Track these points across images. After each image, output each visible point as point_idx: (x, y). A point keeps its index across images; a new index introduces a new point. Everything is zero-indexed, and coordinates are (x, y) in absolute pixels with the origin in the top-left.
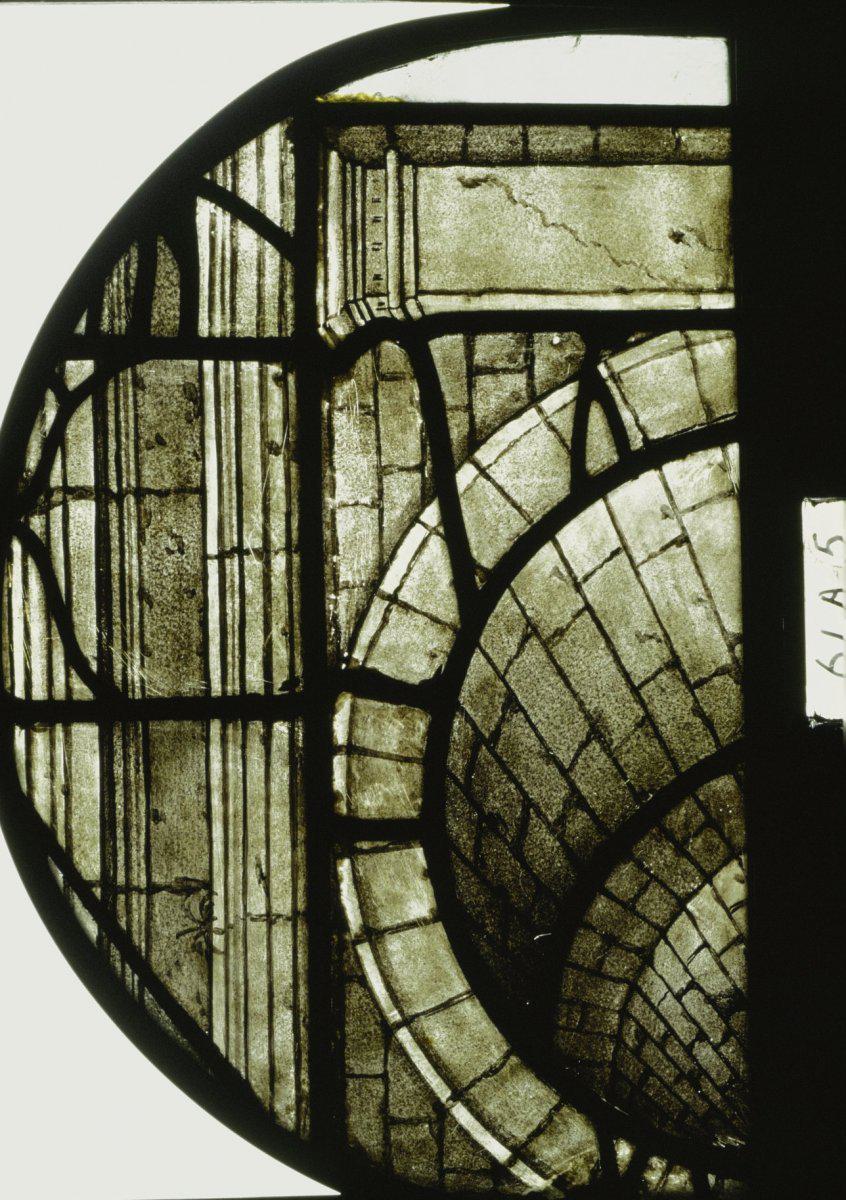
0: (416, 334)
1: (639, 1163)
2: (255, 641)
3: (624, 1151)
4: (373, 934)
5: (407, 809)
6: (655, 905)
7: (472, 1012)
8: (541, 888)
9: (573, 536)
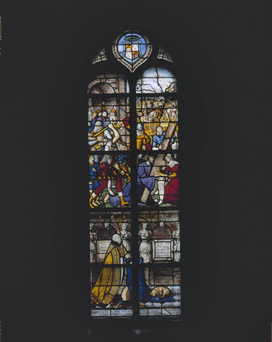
0: (118, 82)
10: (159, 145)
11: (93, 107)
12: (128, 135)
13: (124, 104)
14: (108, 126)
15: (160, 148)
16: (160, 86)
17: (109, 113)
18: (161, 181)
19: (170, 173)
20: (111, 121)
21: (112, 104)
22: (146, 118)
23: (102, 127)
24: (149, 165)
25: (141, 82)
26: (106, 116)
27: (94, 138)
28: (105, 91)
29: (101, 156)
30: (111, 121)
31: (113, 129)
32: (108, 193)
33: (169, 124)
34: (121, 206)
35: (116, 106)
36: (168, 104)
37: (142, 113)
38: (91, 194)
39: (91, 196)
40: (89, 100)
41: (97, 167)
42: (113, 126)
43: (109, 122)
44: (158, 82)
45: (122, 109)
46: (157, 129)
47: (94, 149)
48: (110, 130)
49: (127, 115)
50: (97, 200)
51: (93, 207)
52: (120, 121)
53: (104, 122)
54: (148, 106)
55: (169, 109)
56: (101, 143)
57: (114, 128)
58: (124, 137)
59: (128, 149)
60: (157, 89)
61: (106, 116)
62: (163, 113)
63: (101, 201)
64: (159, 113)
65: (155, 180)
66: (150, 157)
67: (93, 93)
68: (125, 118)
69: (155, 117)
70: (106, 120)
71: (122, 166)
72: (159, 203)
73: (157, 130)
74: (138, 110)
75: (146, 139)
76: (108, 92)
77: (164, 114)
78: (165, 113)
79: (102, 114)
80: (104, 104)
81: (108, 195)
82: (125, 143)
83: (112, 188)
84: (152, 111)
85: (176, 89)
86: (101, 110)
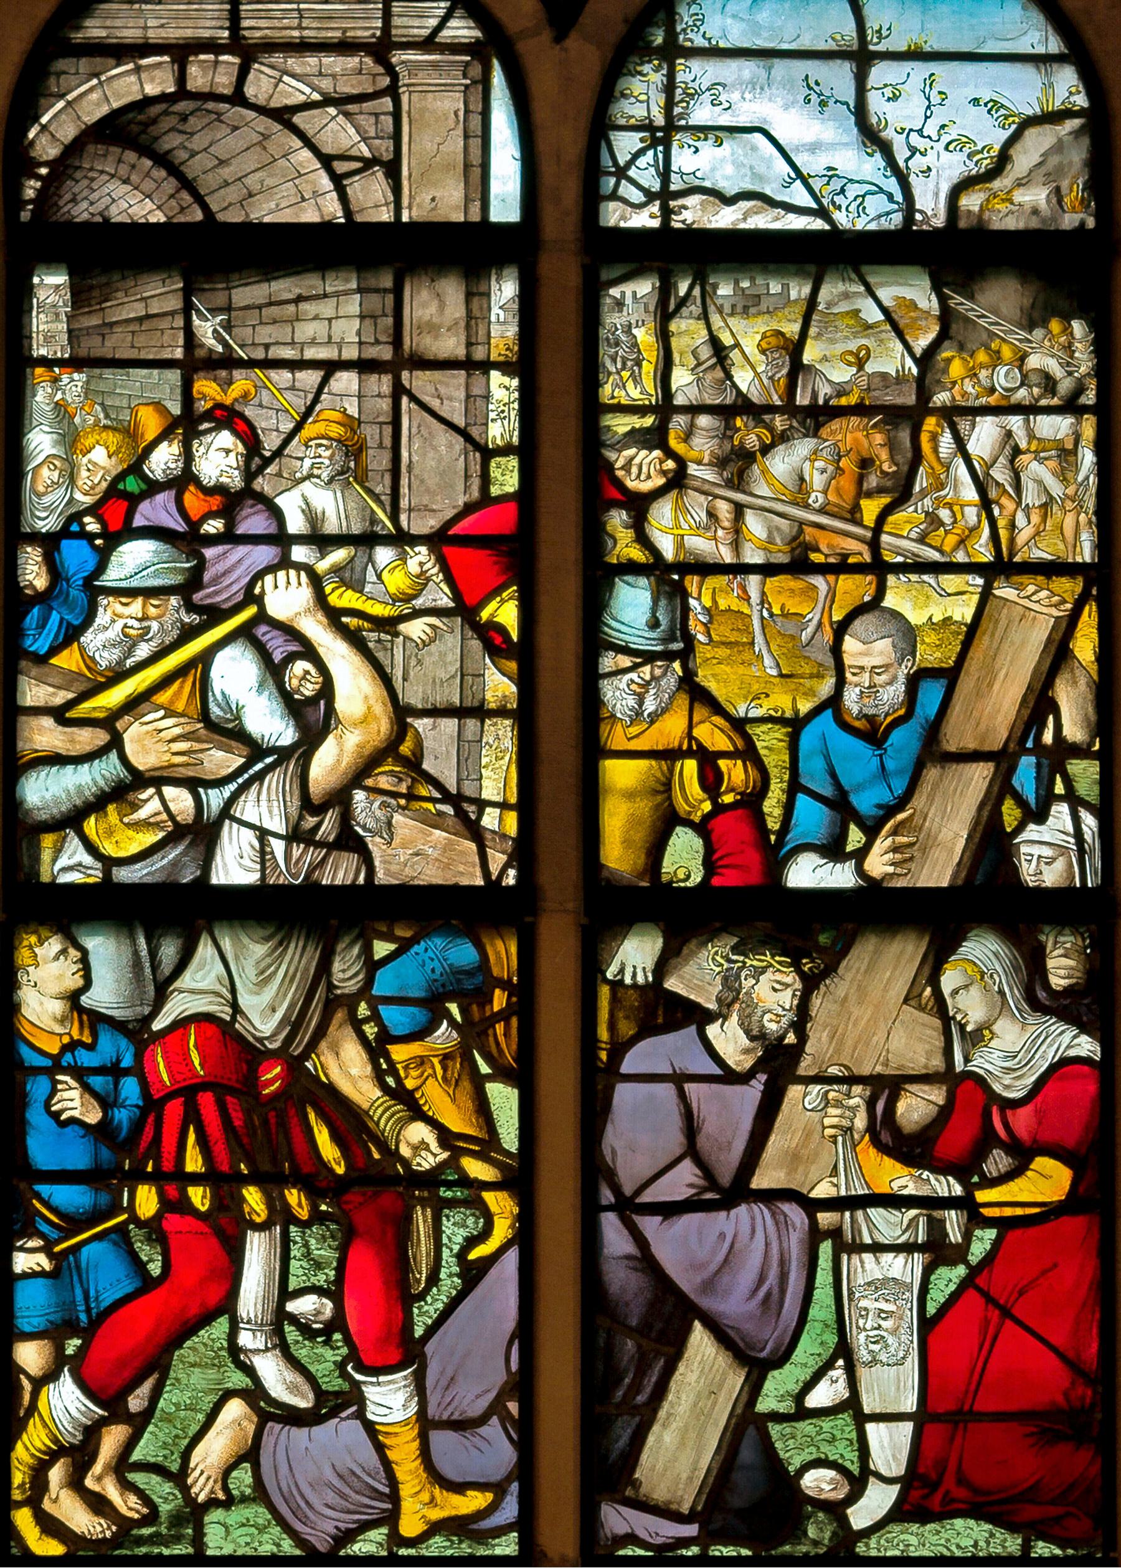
0: (393, 91)
1: (38, 177)
2: (262, 23)
3: (44, 171)
4: (138, 70)
5: (191, 86)
6: (148, 185)
7: (105, 110)
8: (157, 139)
9: (306, 154)
10: (872, 831)
11: (80, 377)
12: (501, 712)
13: (451, 346)
14: (259, 600)
15: (878, 864)
16: (886, 149)
17: (270, 443)
18: (887, 1258)
19: (998, 1161)
20: (300, 539)
21: (313, 342)
22: (712, 514)
23: (190, 607)
24: (748, 1062)
25: (658, 100)
26: (235, 481)
27: (89, 738)
28: (233, 194)
29: (169, 951)
30: (300, 539)
31: (315, 629)
32: (237, 1379)
33: (986, 595)
34: (396, 1539)
35: (364, 366)
36: (982, 357)
37: (670, 453)
38: (35, 1394)
39: (33, 1408)
40: (41, 294)
41: (115, 1071)
42: (321, 599)
43: (265, 554)
44: (860, 112)
45: (435, 404)
46: (850, 644)
47: (88, 860)
48: (279, 648)
49: (486, 480)
50: (97, 1468)
51: (53, 1548)
52: (401, 539)
53: (209, 553)
54: (743, 379)
55: (989, 419)
56: (169, 791)
57: (334, 616)
58: (450, 725)
59: (495, 869)
60: (853, 191)
61: (235, 481)
62: (917, 458)
63: (155, 1479)
64: (865, 463)
65: (815, 1235)
66: (759, 972)
67: (82, 212)
68: (469, 509)
69: (822, 511)
70: (230, 525)
71: (421, 1061)
72: (860, 1516)
73: (848, 660)
74: (621, 425)
75: (707, 760)
76: (266, 212)
77: (933, 474)
78: (947, 467)
79: (188, 456)
80: (210, 341)
81: (235, 1408)
82: (456, 800)
83: (293, 1319)
84: (783, 438)
85: (1075, 189)
86: (176, 409)
